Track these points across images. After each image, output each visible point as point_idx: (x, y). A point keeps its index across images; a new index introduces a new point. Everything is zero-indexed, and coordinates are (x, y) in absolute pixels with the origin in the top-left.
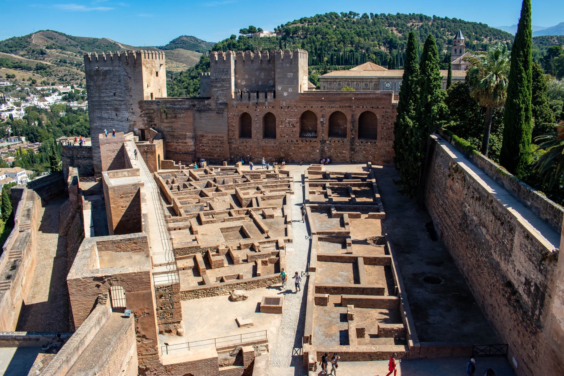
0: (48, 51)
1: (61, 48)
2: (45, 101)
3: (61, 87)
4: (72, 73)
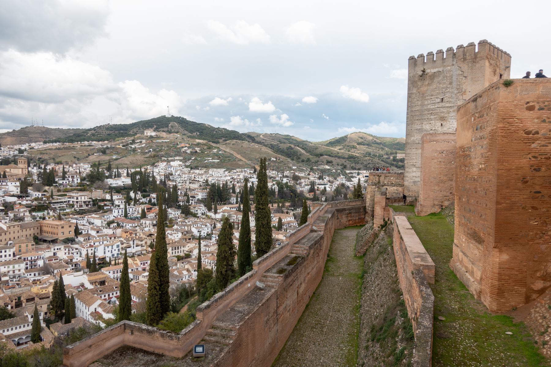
0: (358, 146)
1: (368, 145)
2: (351, 181)
3: (365, 172)
4: (374, 162)
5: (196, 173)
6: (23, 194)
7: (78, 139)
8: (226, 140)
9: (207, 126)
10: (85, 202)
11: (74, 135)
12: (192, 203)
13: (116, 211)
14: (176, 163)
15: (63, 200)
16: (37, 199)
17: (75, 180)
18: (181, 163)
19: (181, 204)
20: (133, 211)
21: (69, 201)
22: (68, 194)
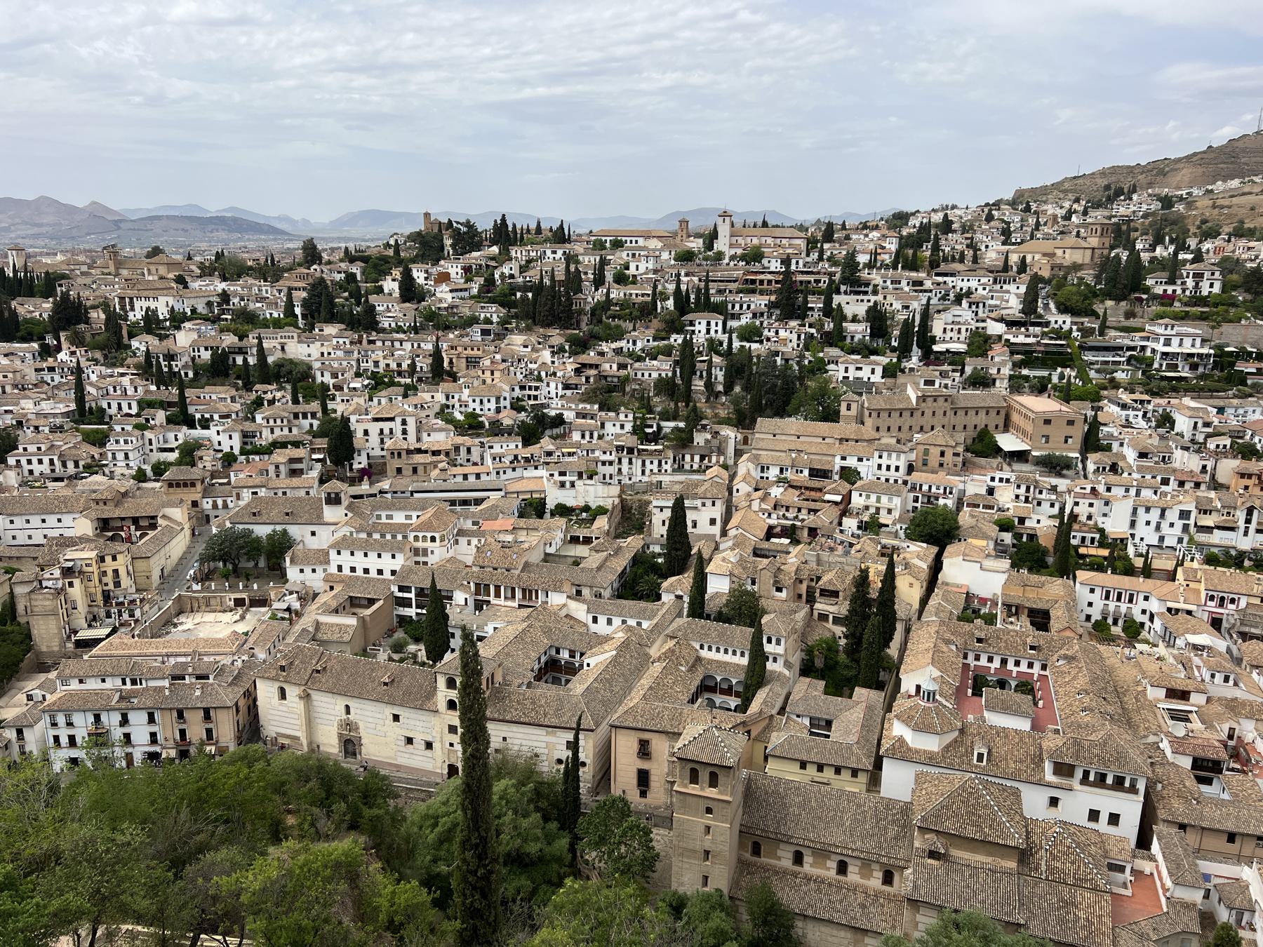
6: (1030, 315)
10: (1192, 355)
15: (1127, 342)
16: (1059, 333)
21: (1143, 348)
22: (1147, 327)
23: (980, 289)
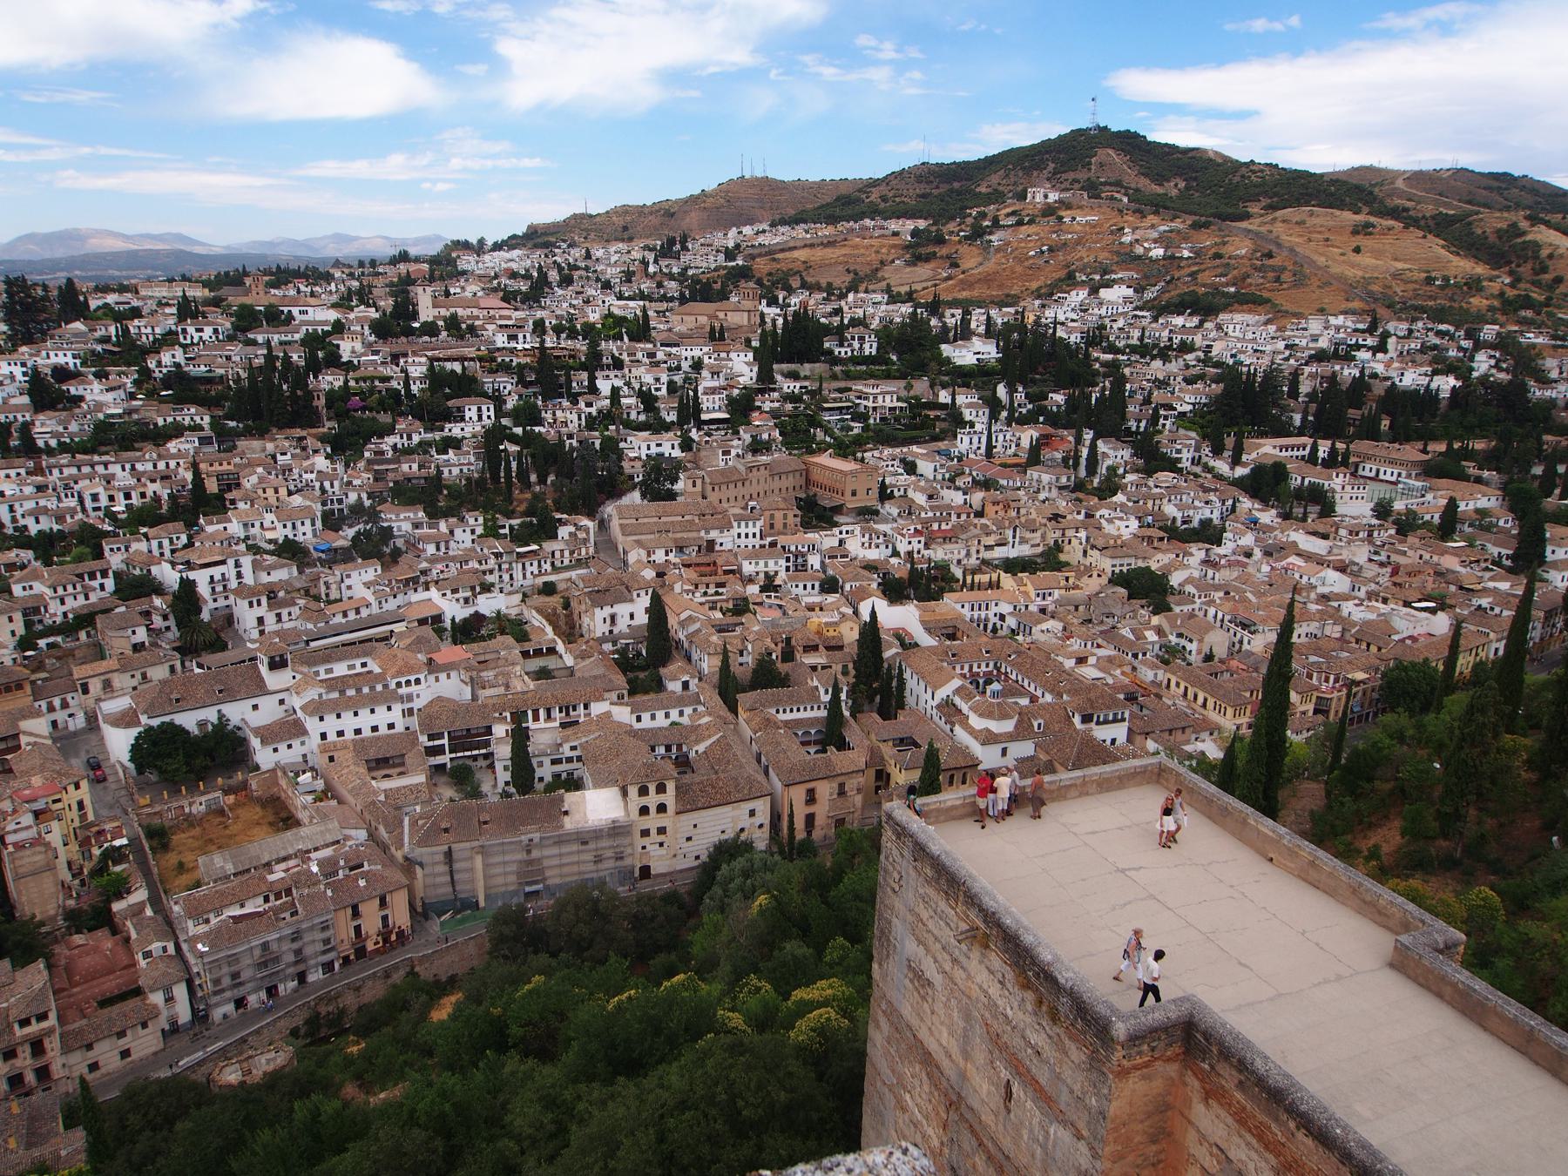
5: (1176, 326)
7: (848, 211)
8: (1272, 208)
9: (1212, 155)
10: (892, 409)
11: (838, 199)
12: (1164, 425)
13: (966, 439)
14: (1115, 295)
17: (867, 346)
18: (1130, 292)
19: (1133, 424)
20: (1005, 441)
23: (706, 357)
